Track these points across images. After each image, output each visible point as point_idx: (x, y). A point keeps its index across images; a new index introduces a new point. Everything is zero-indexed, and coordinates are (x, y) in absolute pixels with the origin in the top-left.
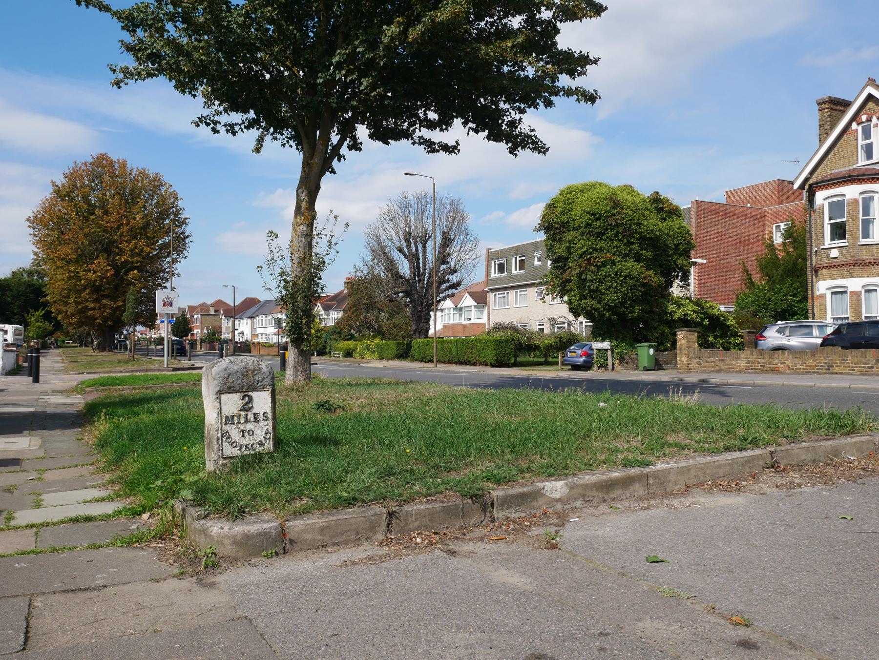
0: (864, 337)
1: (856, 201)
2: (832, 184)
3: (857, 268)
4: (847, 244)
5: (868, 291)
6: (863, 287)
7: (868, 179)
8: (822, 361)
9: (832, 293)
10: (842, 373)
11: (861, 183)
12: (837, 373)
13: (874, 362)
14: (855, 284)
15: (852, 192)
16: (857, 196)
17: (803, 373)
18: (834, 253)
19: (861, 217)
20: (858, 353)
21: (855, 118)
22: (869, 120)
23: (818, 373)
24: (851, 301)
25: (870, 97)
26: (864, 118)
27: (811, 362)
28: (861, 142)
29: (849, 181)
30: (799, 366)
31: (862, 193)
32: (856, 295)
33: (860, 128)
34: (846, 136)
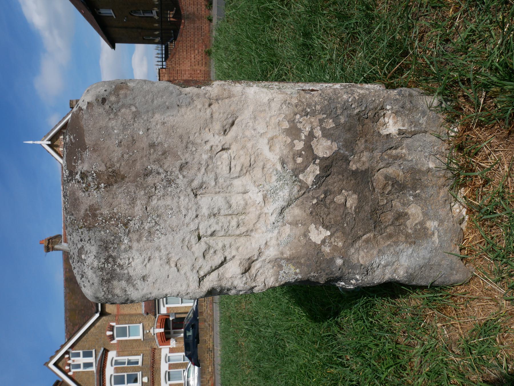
0: (193, 340)
1: (115, 369)
2: (103, 382)
3: (155, 366)
4: (141, 372)
5: (169, 361)
6: (166, 362)
7: (104, 362)
8: (206, 355)
9: (169, 380)
10: (213, 342)
11: (105, 366)
12: (213, 346)
13: (206, 323)
14: (164, 367)
15: (110, 371)
16: (113, 368)
17: (214, 368)
18: (145, 380)
19: (126, 365)
20: (201, 333)
21: (65, 373)
22: (69, 365)
23: (214, 358)
24: (174, 368)
25: (56, 364)
26: (67, 368)
27: (207, 363)
28: (82, 369)
29: (103, 372)
30: (210, 370)
31: (112, 365)
32: (171, 366)
33: (73, 370)
34: (75, 378)
